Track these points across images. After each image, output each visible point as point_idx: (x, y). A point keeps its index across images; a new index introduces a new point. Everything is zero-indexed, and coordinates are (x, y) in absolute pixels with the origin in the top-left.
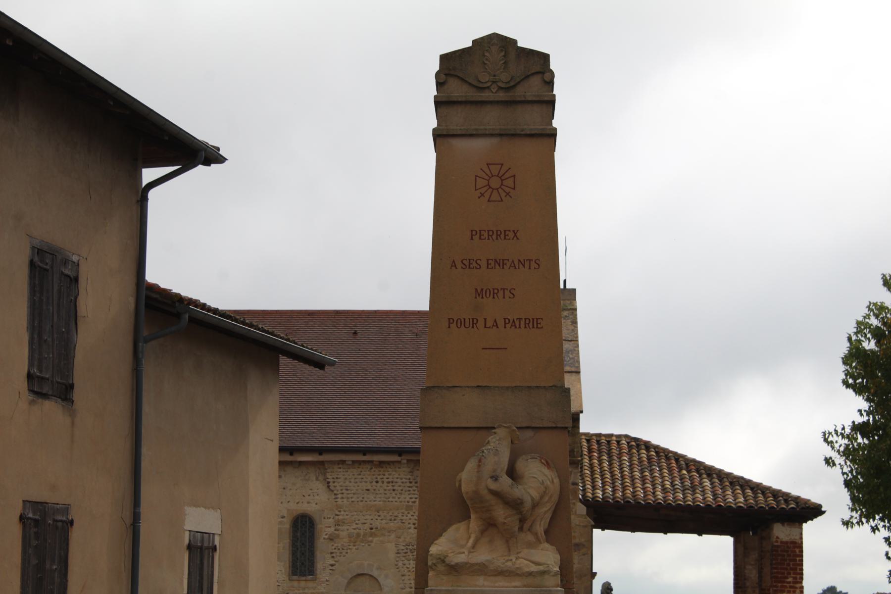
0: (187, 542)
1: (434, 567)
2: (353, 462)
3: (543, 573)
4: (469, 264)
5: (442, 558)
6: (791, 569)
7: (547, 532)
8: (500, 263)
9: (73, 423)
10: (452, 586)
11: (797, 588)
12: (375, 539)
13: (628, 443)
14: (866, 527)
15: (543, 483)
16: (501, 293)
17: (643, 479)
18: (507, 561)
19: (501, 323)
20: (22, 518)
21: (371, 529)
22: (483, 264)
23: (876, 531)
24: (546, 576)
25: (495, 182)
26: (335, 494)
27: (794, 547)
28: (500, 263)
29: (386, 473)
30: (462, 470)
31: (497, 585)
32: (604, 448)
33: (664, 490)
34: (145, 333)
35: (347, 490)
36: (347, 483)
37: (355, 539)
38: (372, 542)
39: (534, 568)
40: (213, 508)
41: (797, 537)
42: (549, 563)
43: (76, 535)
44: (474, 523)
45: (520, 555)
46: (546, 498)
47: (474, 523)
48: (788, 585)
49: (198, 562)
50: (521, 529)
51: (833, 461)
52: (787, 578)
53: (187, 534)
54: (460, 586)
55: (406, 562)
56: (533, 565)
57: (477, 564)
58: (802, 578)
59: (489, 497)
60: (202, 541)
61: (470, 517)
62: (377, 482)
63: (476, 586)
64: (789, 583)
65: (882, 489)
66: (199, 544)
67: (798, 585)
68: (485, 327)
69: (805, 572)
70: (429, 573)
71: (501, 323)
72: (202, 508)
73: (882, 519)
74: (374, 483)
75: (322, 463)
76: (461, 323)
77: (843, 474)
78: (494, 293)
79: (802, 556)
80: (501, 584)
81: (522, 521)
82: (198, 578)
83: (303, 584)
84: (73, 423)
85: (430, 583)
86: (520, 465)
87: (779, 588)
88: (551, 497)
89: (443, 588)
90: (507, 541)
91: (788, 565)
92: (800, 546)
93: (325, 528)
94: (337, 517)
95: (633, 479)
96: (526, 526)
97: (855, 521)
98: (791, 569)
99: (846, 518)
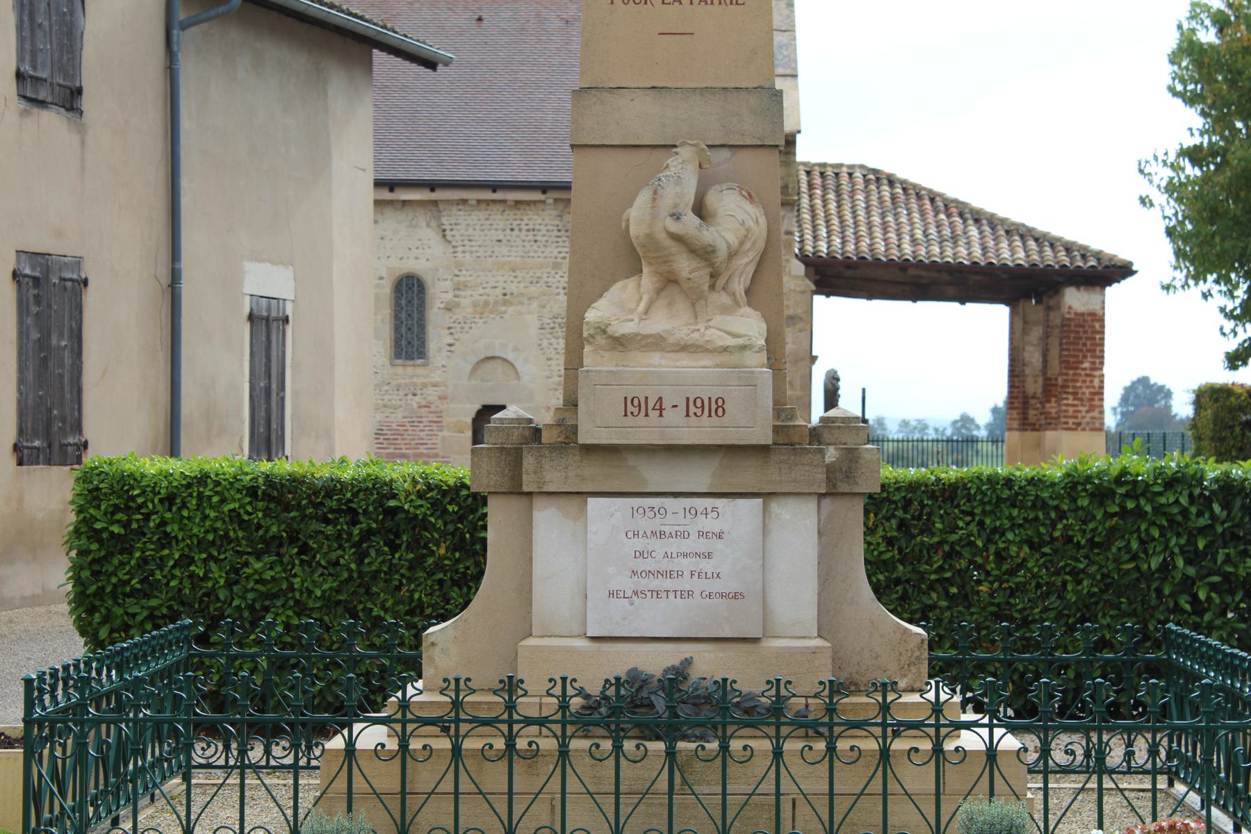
0: (247, 311)
1: (591, 340)
2: (479, 201)
3: (744, 348)
5: (603, 327)
6: (1088, 350)
7: (747, 292)
9: (83, 143)
10: (617, 365)
11: (1094, 376)
12: (511, 310)
13: (864, 176)
14: (1196, 290)
15: (743, 224)
17: (885, 227)
18: (693, 331)
20: (15, 275)
21: (505, 295)
23: (1209, 298)
24: (747, 353)
26: (454, 247)
27: (1093, 321)
29: (525, 218)
30: (630, 203)
31: (679, 364)
32: (831, 182)
33: (914, 241)
34: (181, 15)
35: (470, 240)
36: (470, 231)
37: (483, 308)
38: (505, 312)
39: (730, 342)
40: (282, 264)
41: (1098, 307)
42: (751, 333)
43: (92, 300)
44: (648, 279)
45: (710, 323)
46: (748, 245)
47: (648, 279)
48: (1083, 373)
49: (264, 339)
50: (712, 287)
51: (1150, 201)
52: (1082, 363)
53: (247, 299)
54: (627, 366)
55: (553, 340)
56: (729, 337)
57: (651, 335)
58: (1102, 363)
59: (668, 243)
60: (269, 309)
61: (641, 271)
62: (512, 230)
63: (649, 366)
64: (1085, 369)
65: (1217, 239)
66: (265, 314)
67: (1097, 373)
68: (663, 3)
69: (1106, 355)
70: (583, 348)
72: (268, 265)
73: (1217, 282)
74: (508, 232)
75: (435, 203)
77: (1165, 218)
79: (1103, 333)
80: (684, 363)
81: (714, 276)
82: (264, 360)
83: (410, 370)
84: (83, 143)
85: (586, 361)
86: (712, 199)
87: (1070, 377)
88: (754, 243)
89: (604, 369)
90: (693, 305)
91: (1085, 345)
92: (1101, 320)
93: (439, 294)
94: (456, 279)
95: (870, 226)
96: (720, 283)
97: (1178, 284)
98: (1088, 350)
99: (1166, 281)
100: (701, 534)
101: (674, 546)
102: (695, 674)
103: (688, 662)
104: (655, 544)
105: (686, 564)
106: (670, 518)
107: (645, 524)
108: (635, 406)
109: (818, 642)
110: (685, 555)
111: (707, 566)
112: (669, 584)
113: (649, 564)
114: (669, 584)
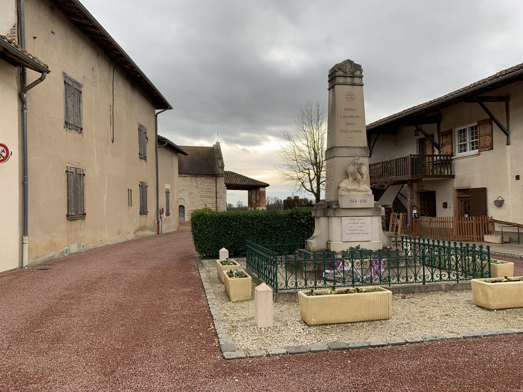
4: (345, 117)
8: (352, 117)
16: (352, 124)
19: (352, 131)
20: (139, 185)
22: (348, 117)
25: (350, 97)
28: (352, 117)
32: (226, 174)
43: (148, 189)
44: (351, 179)
47: (351, 179)
59: (357, 173)
71: (352, 131)
76: (343, 131)
78: (351, 124)
92: (265, 192)
100: (361, 223)
101: (356, 225)
102: (361, 247)
103: (359, 245)
104: (353, 225)
105: (359, 228)
106: (356, 220)
107: (352, 222)
108: (352, 201)
109: (379, 241)
110: (359, 227)
111: (362, 229)
112: (356, 232)
113: (353, 229)
114: (356, 232)
